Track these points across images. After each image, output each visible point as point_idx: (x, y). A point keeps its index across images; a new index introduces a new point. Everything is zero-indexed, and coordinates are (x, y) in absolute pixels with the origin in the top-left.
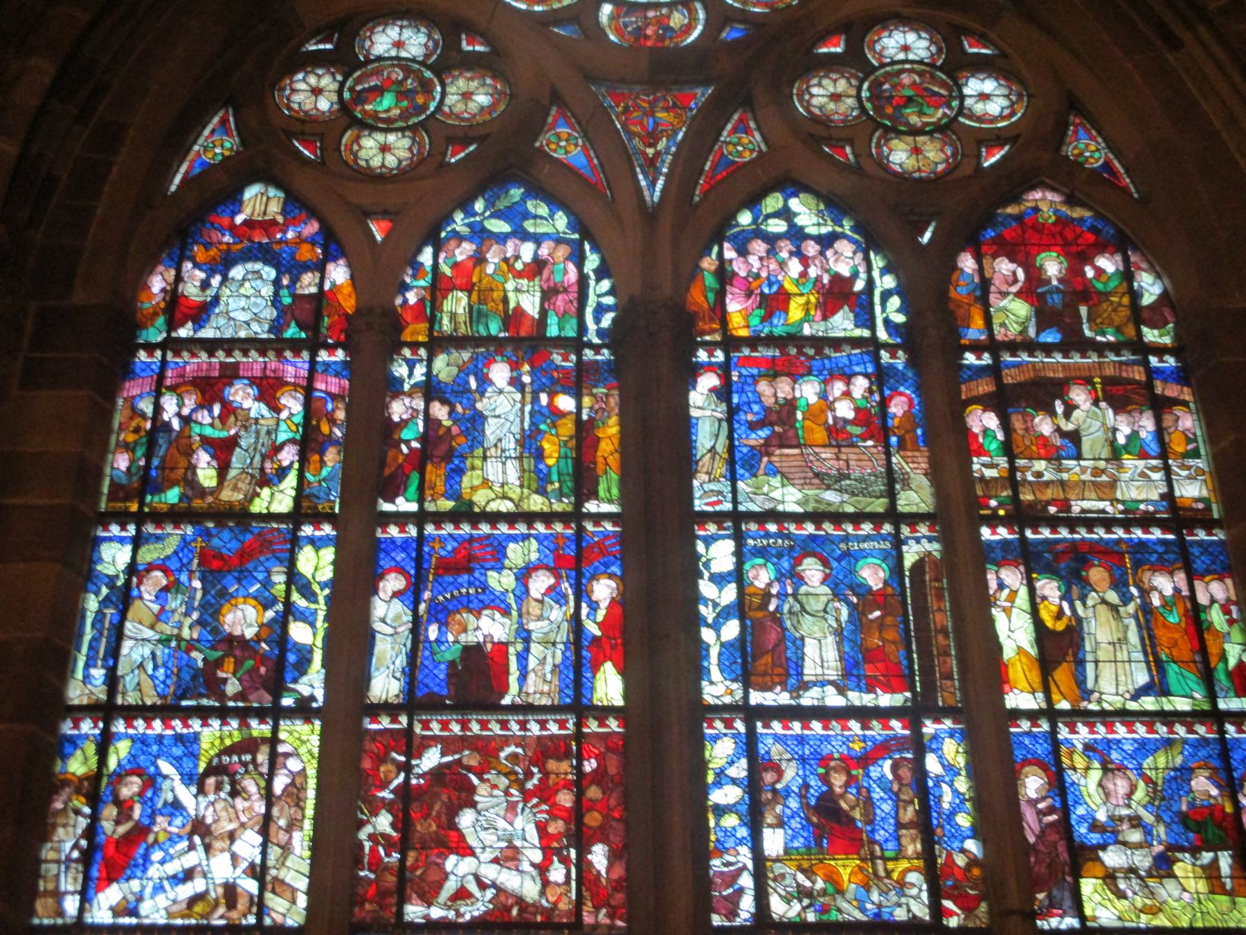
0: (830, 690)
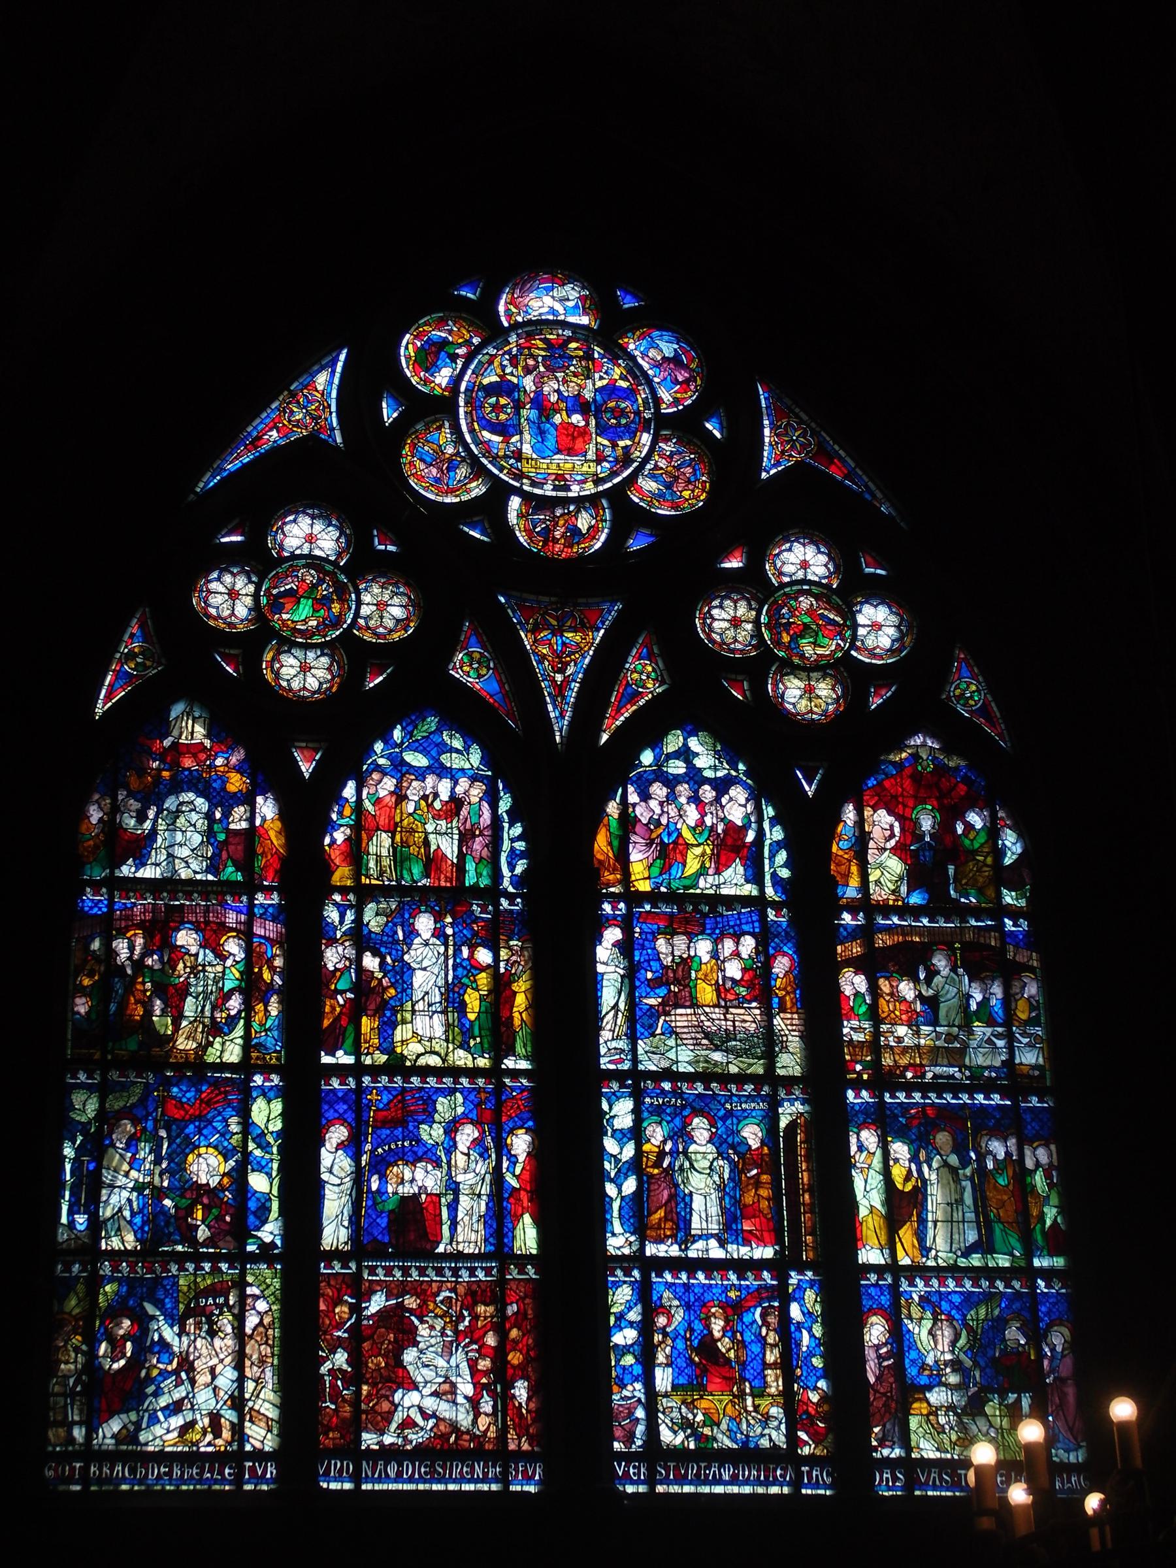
0: (713, 1243)
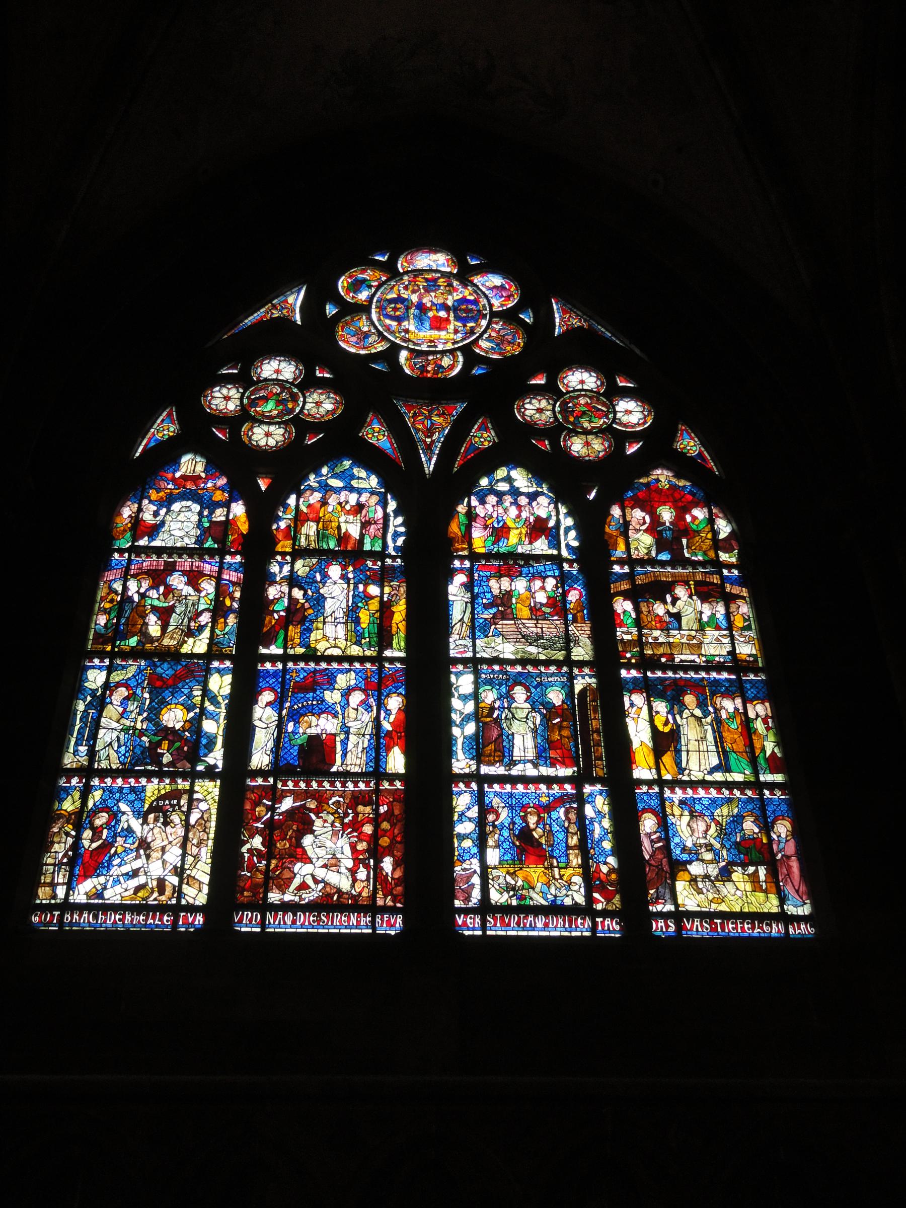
0: (529, 765)
